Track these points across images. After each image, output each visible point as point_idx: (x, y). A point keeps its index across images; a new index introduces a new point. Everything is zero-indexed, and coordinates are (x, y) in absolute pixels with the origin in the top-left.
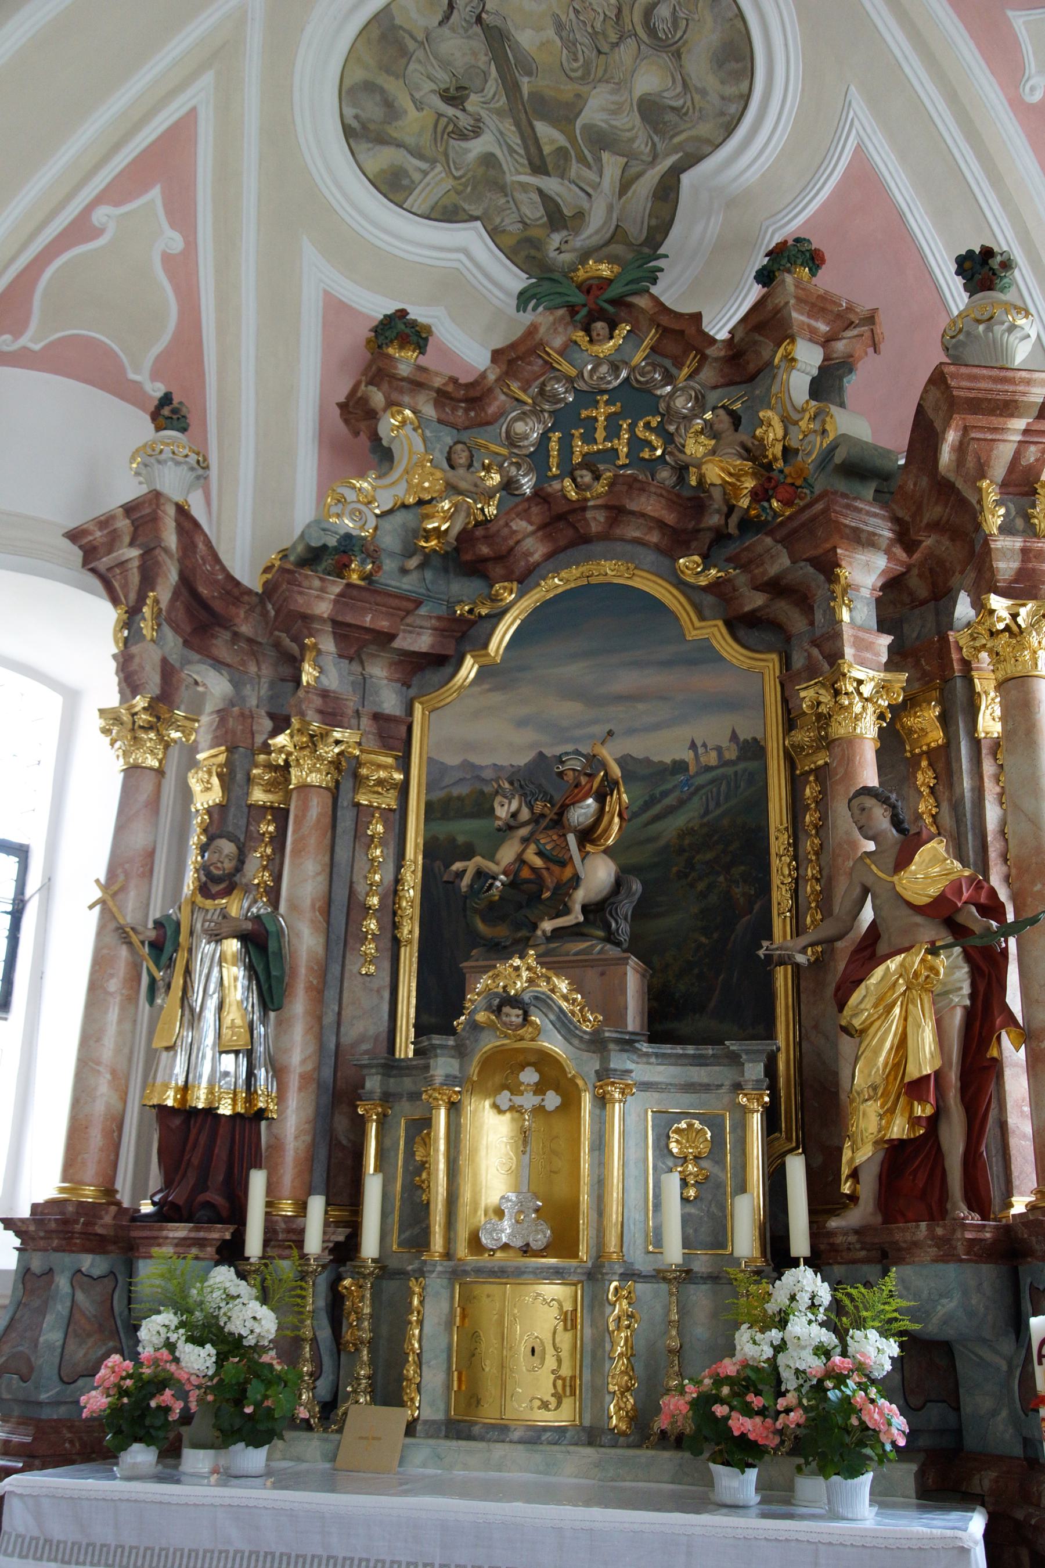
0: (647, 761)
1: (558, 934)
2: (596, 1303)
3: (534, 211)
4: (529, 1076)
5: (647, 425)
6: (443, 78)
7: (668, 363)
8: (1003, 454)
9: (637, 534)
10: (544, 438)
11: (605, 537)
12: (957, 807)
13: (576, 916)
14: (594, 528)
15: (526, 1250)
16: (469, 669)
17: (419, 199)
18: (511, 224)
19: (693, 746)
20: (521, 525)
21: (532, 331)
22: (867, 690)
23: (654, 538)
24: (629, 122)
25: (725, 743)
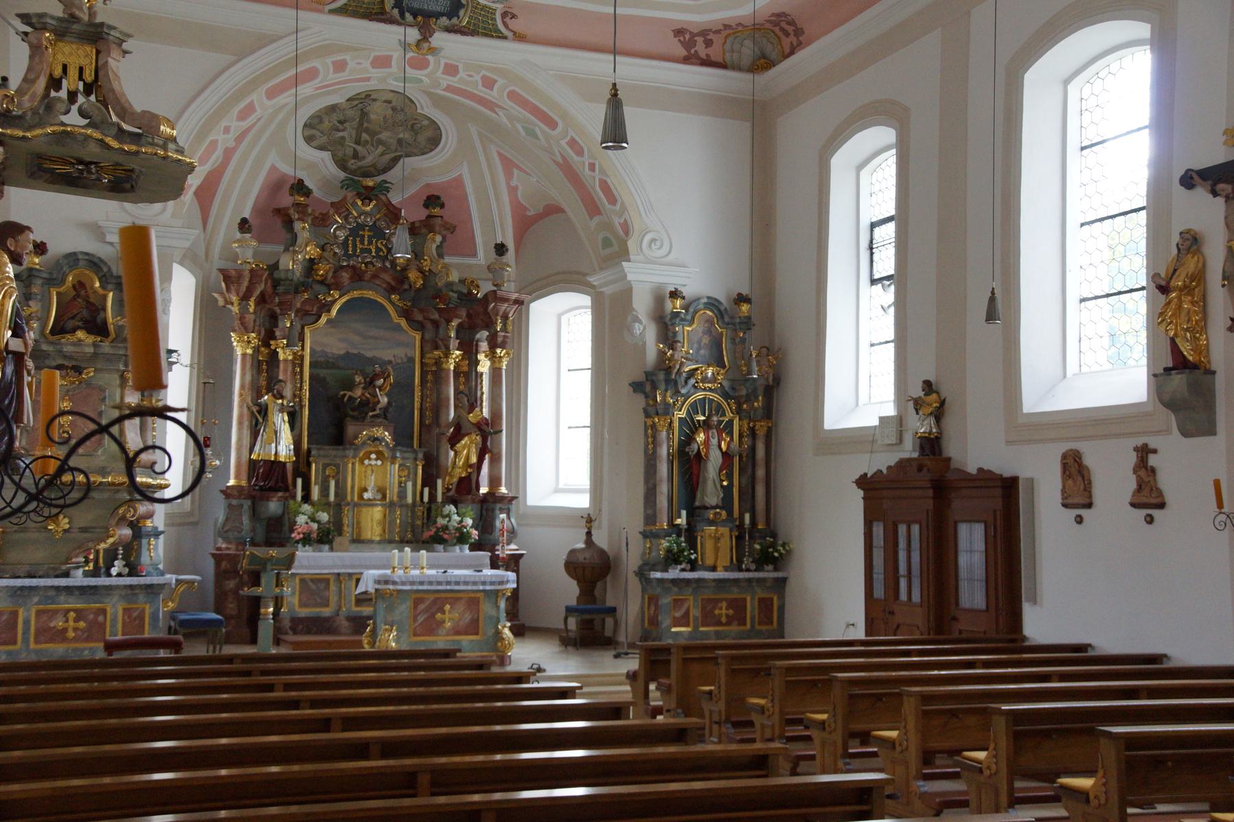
0: (380, 359)
1: (373, 416)
2: (392, 512)
3: (350, 152)
4: (373, 456)
5: (382, 243)
6: (342, 118)
7: (387, 220)
8: (503, 309)
9: (379, 283)
10: (347, 239)
11: (369, 281)
12: (470, 389)
13: (377, 412)
14: (366, 279)
15: (375, 499)
16: (324, 319)
17: (315, 143)
18: (340, 154)
19: (394, 356)
20: (344, 274)
21: (345, 198)
22: (454, 356)
23: (384, 286)
24: (393, 142)
25: (403, 356)
